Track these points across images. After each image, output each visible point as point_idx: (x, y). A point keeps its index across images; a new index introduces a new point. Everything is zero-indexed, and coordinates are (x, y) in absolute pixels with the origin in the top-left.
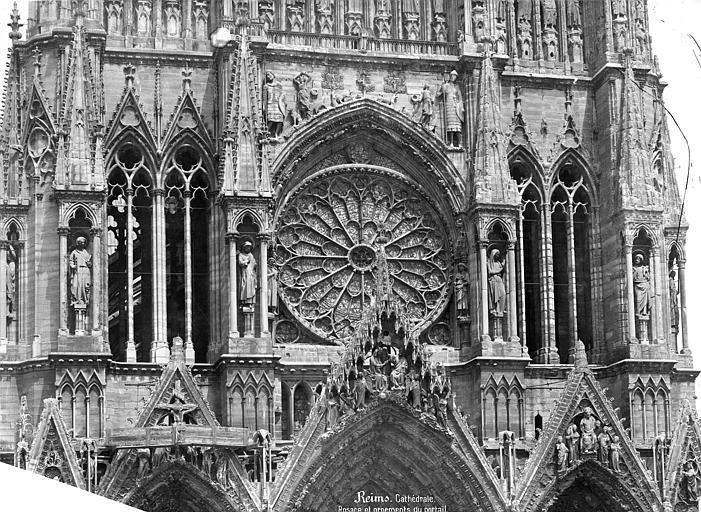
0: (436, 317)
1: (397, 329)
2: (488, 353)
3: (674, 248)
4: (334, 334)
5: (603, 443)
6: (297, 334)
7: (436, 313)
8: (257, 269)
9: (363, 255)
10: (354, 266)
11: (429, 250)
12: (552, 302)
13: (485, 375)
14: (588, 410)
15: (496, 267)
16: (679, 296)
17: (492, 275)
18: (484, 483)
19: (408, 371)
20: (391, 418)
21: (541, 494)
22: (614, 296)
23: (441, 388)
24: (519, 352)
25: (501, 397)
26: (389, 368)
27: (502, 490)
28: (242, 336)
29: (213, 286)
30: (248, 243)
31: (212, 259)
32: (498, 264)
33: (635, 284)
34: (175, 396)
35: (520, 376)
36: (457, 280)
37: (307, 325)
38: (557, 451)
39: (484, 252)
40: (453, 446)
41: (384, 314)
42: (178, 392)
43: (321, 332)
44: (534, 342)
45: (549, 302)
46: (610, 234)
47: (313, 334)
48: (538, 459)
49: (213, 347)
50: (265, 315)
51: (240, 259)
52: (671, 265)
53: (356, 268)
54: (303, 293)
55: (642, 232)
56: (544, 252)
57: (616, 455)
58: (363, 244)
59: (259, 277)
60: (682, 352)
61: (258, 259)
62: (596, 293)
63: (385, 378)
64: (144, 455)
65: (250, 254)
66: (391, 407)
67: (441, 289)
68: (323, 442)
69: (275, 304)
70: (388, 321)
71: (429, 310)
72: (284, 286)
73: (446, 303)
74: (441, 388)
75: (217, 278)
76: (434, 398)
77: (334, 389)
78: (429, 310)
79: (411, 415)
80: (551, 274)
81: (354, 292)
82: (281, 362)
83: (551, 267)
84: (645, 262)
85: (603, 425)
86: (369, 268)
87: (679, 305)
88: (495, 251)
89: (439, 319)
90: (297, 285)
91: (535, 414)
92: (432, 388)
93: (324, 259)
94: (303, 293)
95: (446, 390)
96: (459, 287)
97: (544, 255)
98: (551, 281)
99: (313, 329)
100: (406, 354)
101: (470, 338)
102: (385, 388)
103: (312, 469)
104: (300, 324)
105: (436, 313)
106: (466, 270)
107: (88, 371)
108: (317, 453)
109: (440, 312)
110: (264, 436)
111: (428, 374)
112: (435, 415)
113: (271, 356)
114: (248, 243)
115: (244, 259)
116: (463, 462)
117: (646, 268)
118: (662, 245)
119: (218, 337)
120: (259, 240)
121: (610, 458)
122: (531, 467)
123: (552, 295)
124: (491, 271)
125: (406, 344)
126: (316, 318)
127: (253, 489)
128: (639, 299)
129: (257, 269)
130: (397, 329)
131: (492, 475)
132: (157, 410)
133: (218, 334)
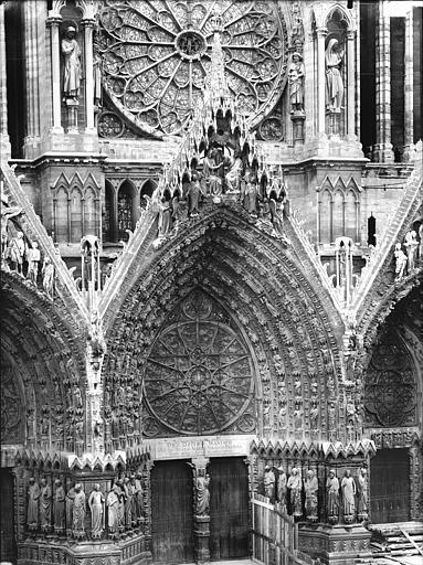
0: (268, 111)
1: (233, 128)
2: (324, 153)
4: (159, 128)
6: (121, 127)
8: (82, 58)
9: (191, 41)
10: (182, 54)
11: (261, 37)
12: (388, 94)
15: (334, 60)
17: (330, 67)
19: (243, 173)
20: (225, 223)
21: (377, 304)
23: (278, 193)
24: (352, 149)
26: (222, 173)
28: (66, 131)
29: (30, 73)
30: (71, 29)
31: (28, 43)
32: (335, 56)
35: (356, 175)
36: (291, 71)
37: (131, 118)
38: (395, 259)
39: (322, 41)
41: (220, 112)
43: (147, 128)
44: (369, 137)
45: (384, 96)
47: (138, 128)
48: (375, 267)
49: (31, 141)
50: (91, 108)
51: (64, 47)
53: (184, 56)
54: (128, 82)
56: (381, 40)
58: (191, 30)
59: (83, 67)
61: (83, 46)
63: (220, 181)
65: (74, 41)
66: (225, 211)
67: (273, 80)
69: (99, 96)
70: (223, 119)
71: (261, 103)
72: (107, 74)
73: (279, 96)
74: (278, 193)
75: (35, 64)
76: (270, 202)
77: (167, 193)
78: (261, 103)
80: (388, 64)
81: (181, 82)
82: (106, 160)
83: (388, 56)
86: (197, 56)
88: (333, 41)
89: (270, 114)
90: (120, 74)
91: (369, 216)
92: (269, 192)
93: (148, 45)
94: (128, 82)
95: (283, 194)
96: (293, 79)
97: (381, 43)
98: (388, 71)
99: (139, 123)
101: (303, 135)
102: (218, 191)
103: (144, 276)
104: (126, 119)
105: (268, 106)
106: (301, 60)
108: (149, 260)
110: (92, 243)
111: (264, 177)
112: (272, 221)
113: (98, 155)
114: (71, 29)
115: (67, 46)
119: (36, 131)
120: (83, 25)
122: (369, 275)
123: (388, 87)
125: (242, 144)
126: (141, 111)
129: (82, 58)
130: (233, 128)
131: (327, 282)
133: (36, 126)
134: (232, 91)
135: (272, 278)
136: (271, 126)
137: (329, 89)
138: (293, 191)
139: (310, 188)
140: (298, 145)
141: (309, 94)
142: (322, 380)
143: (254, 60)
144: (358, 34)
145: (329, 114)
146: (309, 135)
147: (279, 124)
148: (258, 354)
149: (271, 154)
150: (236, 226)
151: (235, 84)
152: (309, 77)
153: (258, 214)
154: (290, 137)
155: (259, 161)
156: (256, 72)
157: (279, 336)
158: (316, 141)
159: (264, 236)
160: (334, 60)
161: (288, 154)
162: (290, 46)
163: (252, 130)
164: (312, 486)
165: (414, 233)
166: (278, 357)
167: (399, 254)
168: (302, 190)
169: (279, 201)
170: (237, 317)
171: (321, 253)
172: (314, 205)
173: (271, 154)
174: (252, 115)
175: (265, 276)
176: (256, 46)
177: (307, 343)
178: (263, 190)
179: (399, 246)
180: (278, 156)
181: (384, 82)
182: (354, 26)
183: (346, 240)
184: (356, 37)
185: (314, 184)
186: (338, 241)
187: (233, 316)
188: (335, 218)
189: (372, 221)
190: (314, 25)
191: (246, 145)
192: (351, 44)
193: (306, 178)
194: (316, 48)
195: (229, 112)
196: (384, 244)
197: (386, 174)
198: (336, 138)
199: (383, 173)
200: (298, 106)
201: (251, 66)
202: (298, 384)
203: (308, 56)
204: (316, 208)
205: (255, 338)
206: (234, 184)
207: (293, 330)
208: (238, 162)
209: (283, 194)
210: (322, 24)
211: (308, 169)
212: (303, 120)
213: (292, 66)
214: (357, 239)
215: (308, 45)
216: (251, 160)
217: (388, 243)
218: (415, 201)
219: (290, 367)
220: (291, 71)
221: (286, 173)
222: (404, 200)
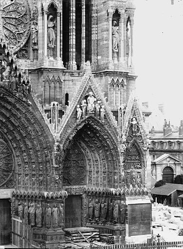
0: (22, 46)
1: (6, 52)
2: (46, 65)
3: (129, 18)
7: (22, 43)
11: (19, 13)
12: (74, 40)
14: (91, 93)
15: (51, 24)
16: (130, 40)
17: (49, 27)
19: (10, 73)
20: (2, 94)
22: (102, 39)
23: (26, 82)
24: (59, 64)
32: (52, 23)
33: (113, 34)
35: (61, 75)
36: (32, 28)
38: (77, 112)
39: (46, 16)
44: (66, 59)
52: (127, 26)
55: (117, 11)
60: (130, 66)
62: (94, 37)
66: (2, 89)
71: (19, 42)
73: (27, 39)
74: (26, 82)
76: (22, 85)
78: (19, 42)
79: (12, 93)
80: (74, 27)
83: (74, 24)
84: (117, 25)
85: (97, 100)
87: (130, 44)
88: (51, 16)
89: (23, 47)
91: (66, 93)
92: (22, 81)
95: (28, 82)
96: (33, 32)
97: (71, 18)
98: (74, 30)
100: (11, 64)
101: (37, 56)
105: (22, 43)
106: (37, 24)
109: (24, 43)
111: (20, 75)
112: (23, 94)
117: (117, 28)
118: (123, 17)
121: (100, 115)
122: (65, 119)
123: (74, 37)
124: (49, 26)
125: (10, 60)
128: (114, 42)
130: (6, 52)
131: (47, 121)
134: (6, 37)
135: (23, 119)
136: (23, 52)
137: (49, 37)
138: (33, 81)
139: (40, 80)
140: (35, 61)
141: (40, 39)
142: (45, 164)
143: (16, 23)
144: (62, 14)
145: (48, 48)
146: (40, 57)
147: (27, 52)
148: (16, 153)
149: (23, 65)
150: (7, 95)
151: (7, 33)
152: (40, 31)
153: (17, 91)
154: (31, 57)
155: (18, 67)
156: (17, 28)
157: (26, 145)
158: (43, 59)
159: (19, 100)
160: (51, 24)
161: (31, 65)
162: (32, 18)
163: (14, 54)
164: (39, 211)
165: (85, 101)
166: (25, 154)
167: (79, 110)
168: (37, 81)
169: (26, 85)
170: (7, 136)
171: (45, 108)
172: (42, 87)
173: (23, 65)
174: (15, 47)
175: (20, 118)
176: (17, 17)
177: (38, 148)
178: (20, 80)
179: (78, 106)
180: (26, 65)
181: (73, 35)
182: (60, 10)
183: (56, 103)
184: (61, 15)
185: (42, 79)
186: (52, 103)
187: (5, 136)
188: (51, 93)
189: (67, 95)
190: (42, 9)
191: (12, 60)
192: (58, 18)
193: (38, 75)
194: (43, 19)
195: (4, 45)
196: (72, 106)
197: (73, 75)
198: (52, 59)
199: (72, 75)
200: (35, 44)
201: (15, 26)
202: (34, 166)
203: (40, 22)
204: (43, 89)
205: (15, 145)
206: (6, 77)
207: (32, 142)
208: (9, 67)
209: (28, 82)
210: (46, 8)
211: (40, 71)
212: (37, 50)
213: (33, 26)
214: (61, 103)
215: (40, 18)
216: (14, 67)
217: (74, 105)
218: (86, 87)
219: (30, 158)
220: (32, 28)
221: (30, 73)
222: (81, 86)
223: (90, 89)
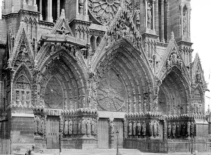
5: (179, 61)
13: (147, 38)
14: (175, 51)
18: (148, 69)
25: (150, 46)
27: (153, 71)
34: (62, 27)
38: (167, 62)
40: (141, 56)
42: (63, 26)
46: (175, 6)
57: (182, 65)
64: (53, 45)
68: (106, 49)
86: (112, 4)
107: (33, 17)
116: (143, 62)
122: (161, 66)
127: (86, 61)
132: (57, 31)
159: (135, 50)
205: (127, 84)
223: (174, 49)
